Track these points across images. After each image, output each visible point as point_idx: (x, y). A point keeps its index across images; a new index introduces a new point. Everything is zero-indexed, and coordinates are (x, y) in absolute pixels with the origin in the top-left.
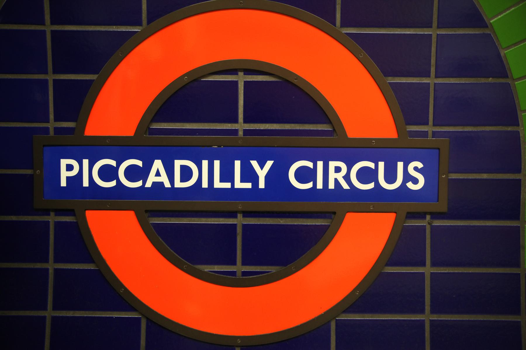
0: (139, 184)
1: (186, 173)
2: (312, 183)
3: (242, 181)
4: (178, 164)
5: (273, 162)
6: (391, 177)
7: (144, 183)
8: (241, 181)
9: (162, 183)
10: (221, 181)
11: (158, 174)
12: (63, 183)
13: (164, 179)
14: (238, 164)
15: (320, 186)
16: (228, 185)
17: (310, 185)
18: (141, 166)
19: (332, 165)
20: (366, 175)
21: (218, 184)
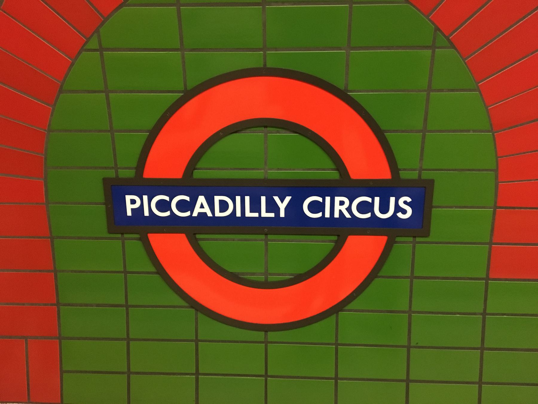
0: (188, 214)
1: (224, 206)
2: (321, 213)
3: (267, 211)
4: (217, 199)
5: (291, 197)
6: (384, 209)
7: (192, 213)
10: (251, 212)
11: (202, 206)
12: (129, 213)
13: (207, 210)
14: (263, 199)
16: (256, 215)
17: (319, 215)
18: (189, 200)
19: (337, 199)
20: (364, 207)
21: (248, 214)
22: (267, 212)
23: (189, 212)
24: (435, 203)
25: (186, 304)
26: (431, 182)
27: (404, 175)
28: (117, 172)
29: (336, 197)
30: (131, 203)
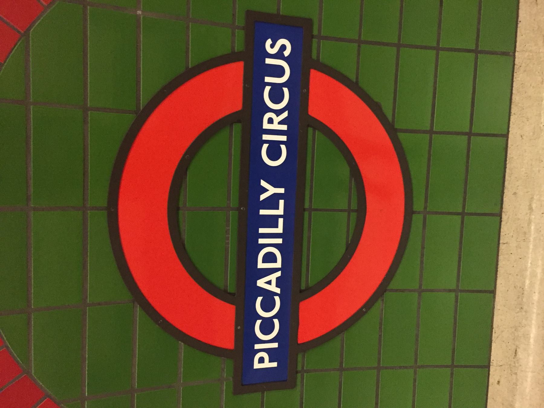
0: (277, 299)
1: (270, 258)
4: (261, 265)
5: (262, 180)
6: (280, 72)
9: (278, 279)
11: (269, 283)
12: (275, 365)
13: (273, 277)
14: (263, 212)
15: (284, 138)
16: (281, 221)
17: (283, 147)
18: (261, 298)
19: (266, 126)
21: (280, 230)
22: (277, 227)
23: (275, 297)
24: (275, 12)
26: (249, 14)
27: (239, 46)
29: (264, 128)
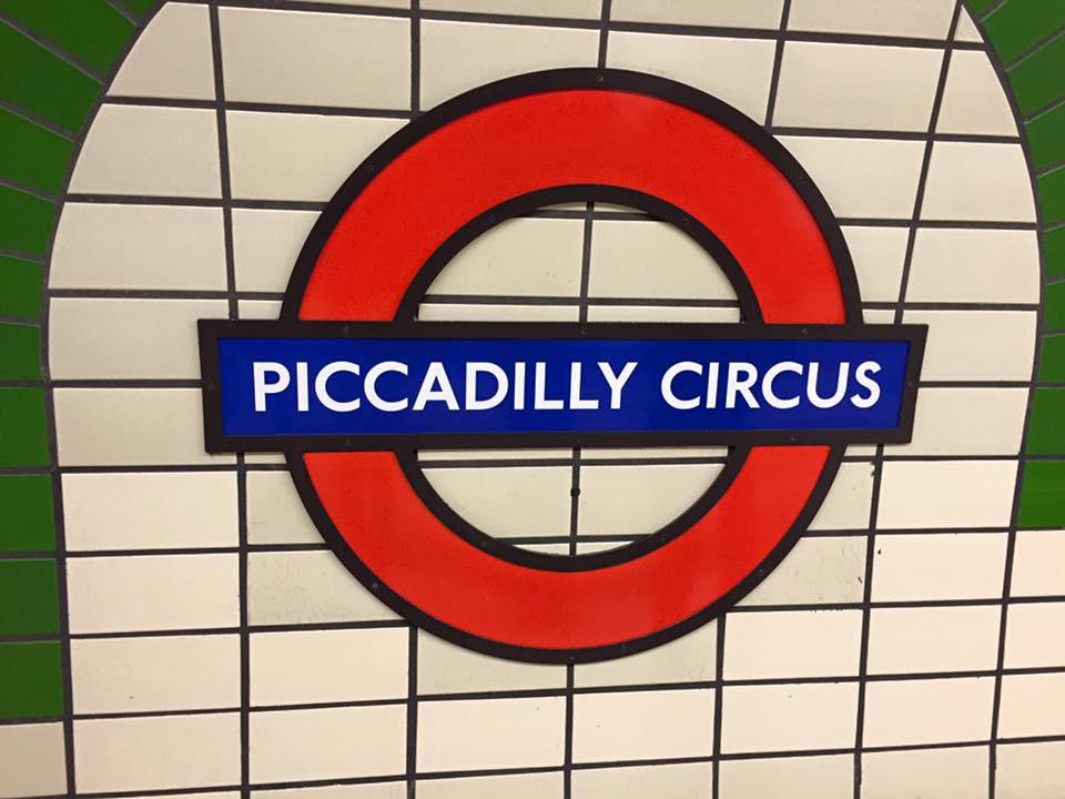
0: (402, 404)
1: (486, 385)
4: (472, 369)
5: (636, 364)
6: (826, 389)
7: (412, 403)
8: (547, 398)
9: (443, 403)
11: (436, 387)
12: (260, 406)
13: (447, 395)
14: (576, 368)
15: (711, 403)
16: (558, 405)
17: (695, 402)
18: (406, 373)
19: (734, 368)
20: (786, 385)
21: (541, 403)
23: (406, 400)
24: (924, 378)
25: (391, 616)
26: (921, 331)
28: (234, 309)
29: (731, 364)
30: (265, 381)
